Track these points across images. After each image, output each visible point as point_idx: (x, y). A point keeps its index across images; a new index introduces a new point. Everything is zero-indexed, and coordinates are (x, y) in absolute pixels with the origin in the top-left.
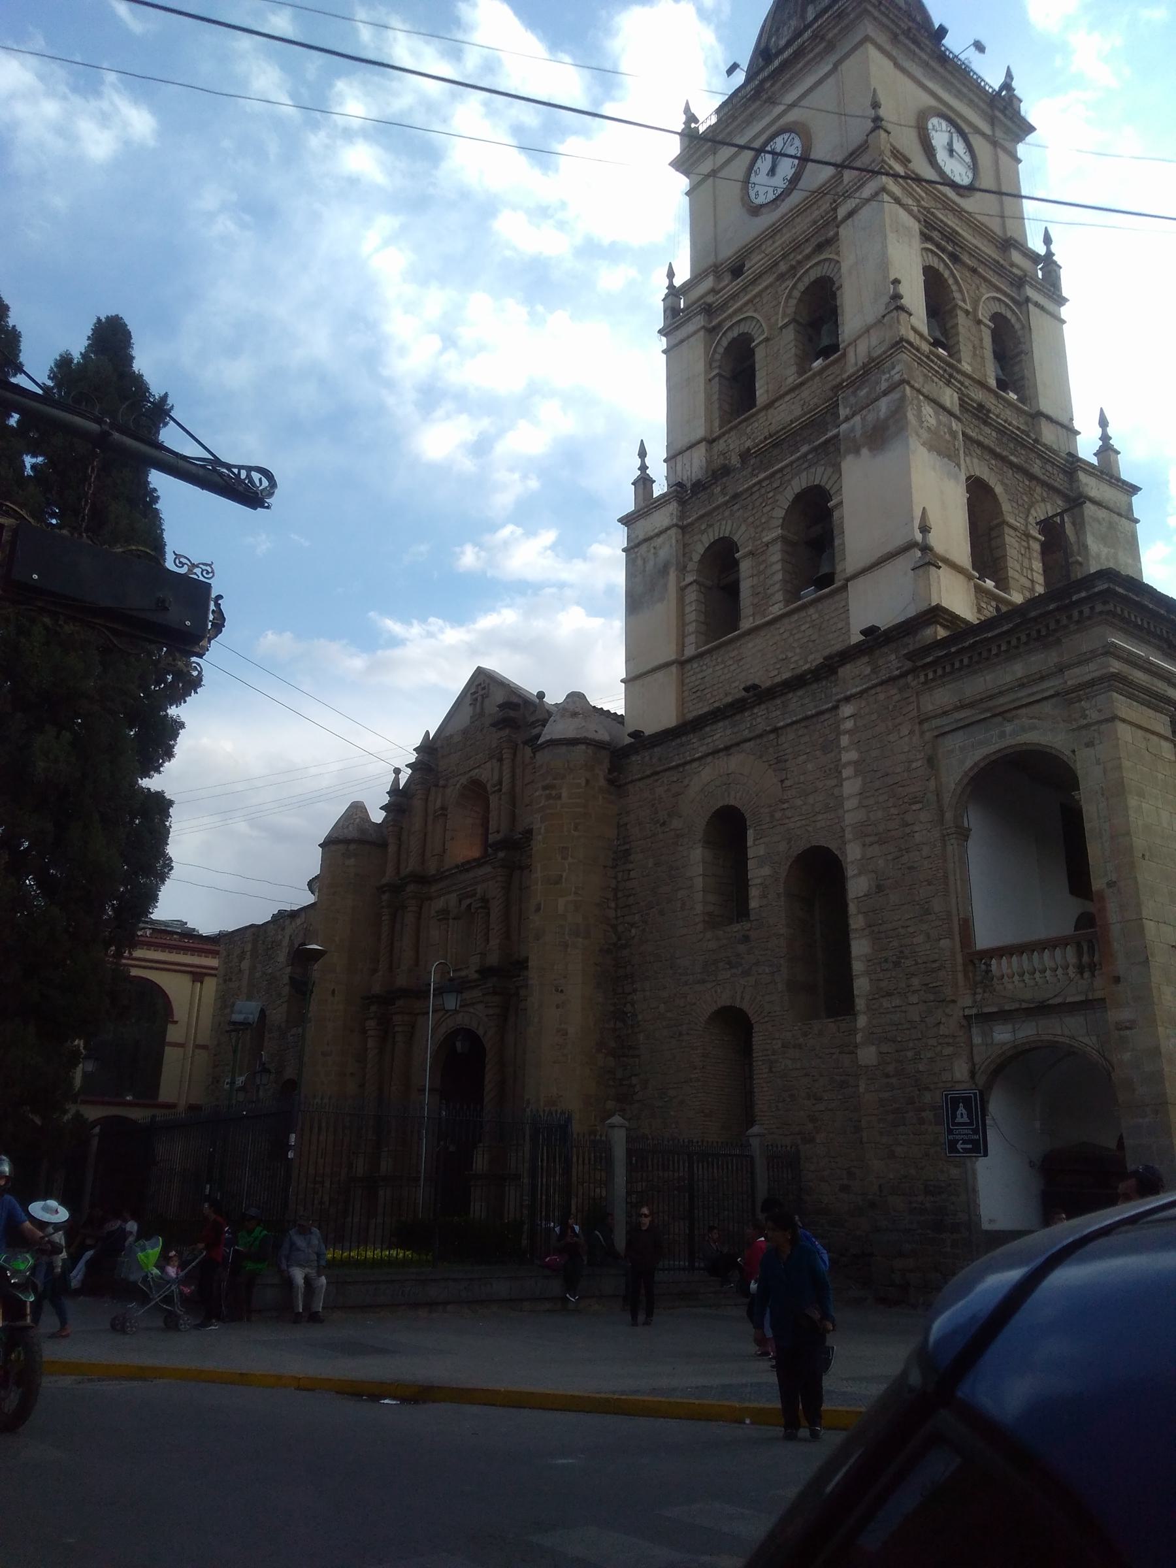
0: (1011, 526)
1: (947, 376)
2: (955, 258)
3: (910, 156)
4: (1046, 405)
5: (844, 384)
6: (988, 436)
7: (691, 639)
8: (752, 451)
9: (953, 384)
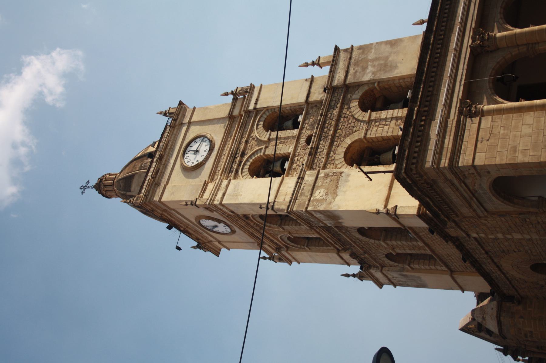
0: (366, 134)
1: (300, 180)
2: (243, 154)
3: (203, 182)
4: (302, 99)
5: (309, 225)
6: (324, 146)
7: (439, 268)
8: (343, 248)
9: (303, 175)
